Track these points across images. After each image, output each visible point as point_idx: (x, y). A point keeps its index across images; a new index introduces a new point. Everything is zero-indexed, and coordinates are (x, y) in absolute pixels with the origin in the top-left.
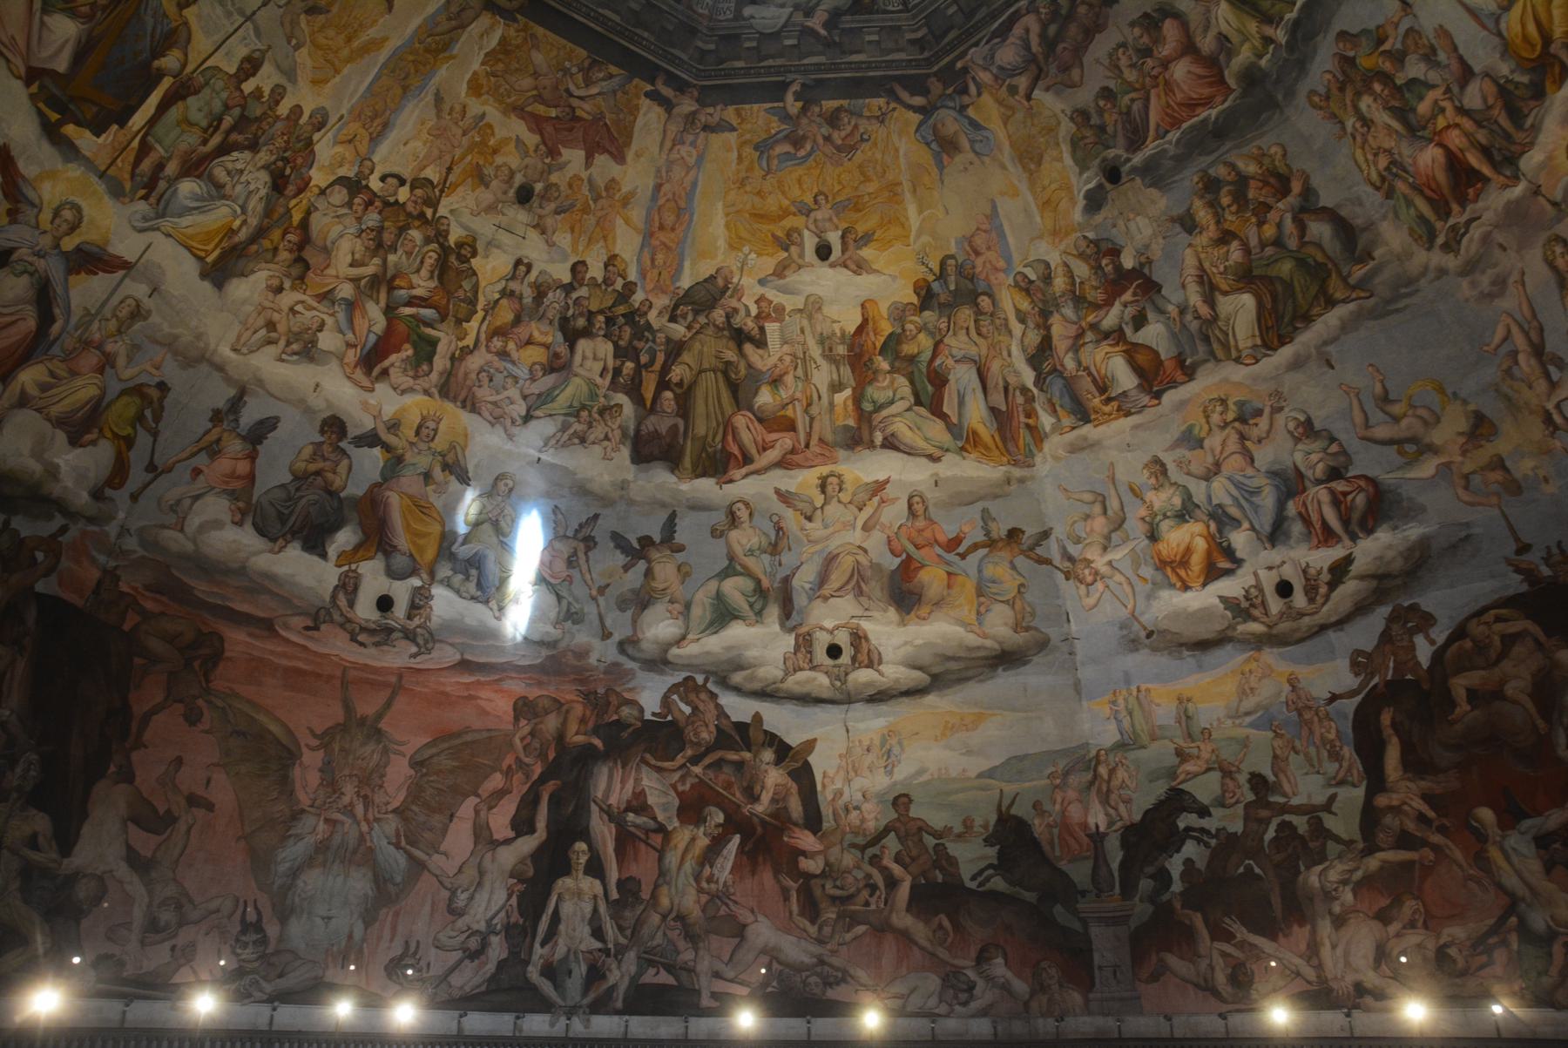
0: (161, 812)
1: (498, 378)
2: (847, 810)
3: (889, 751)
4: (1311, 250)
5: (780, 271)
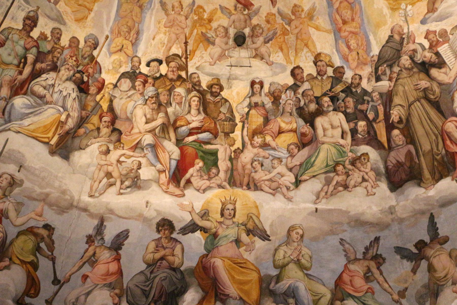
1: (267, 162)
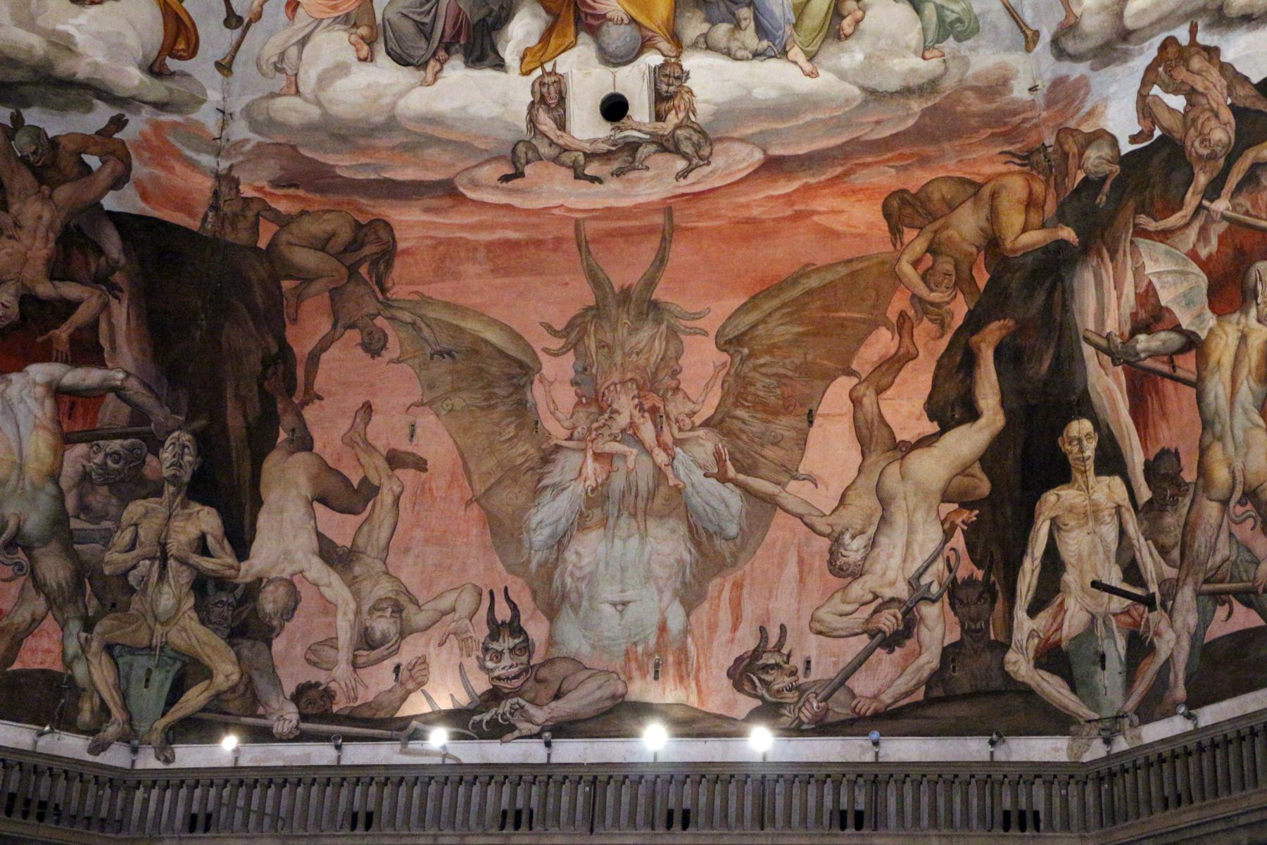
0: (356, 485)
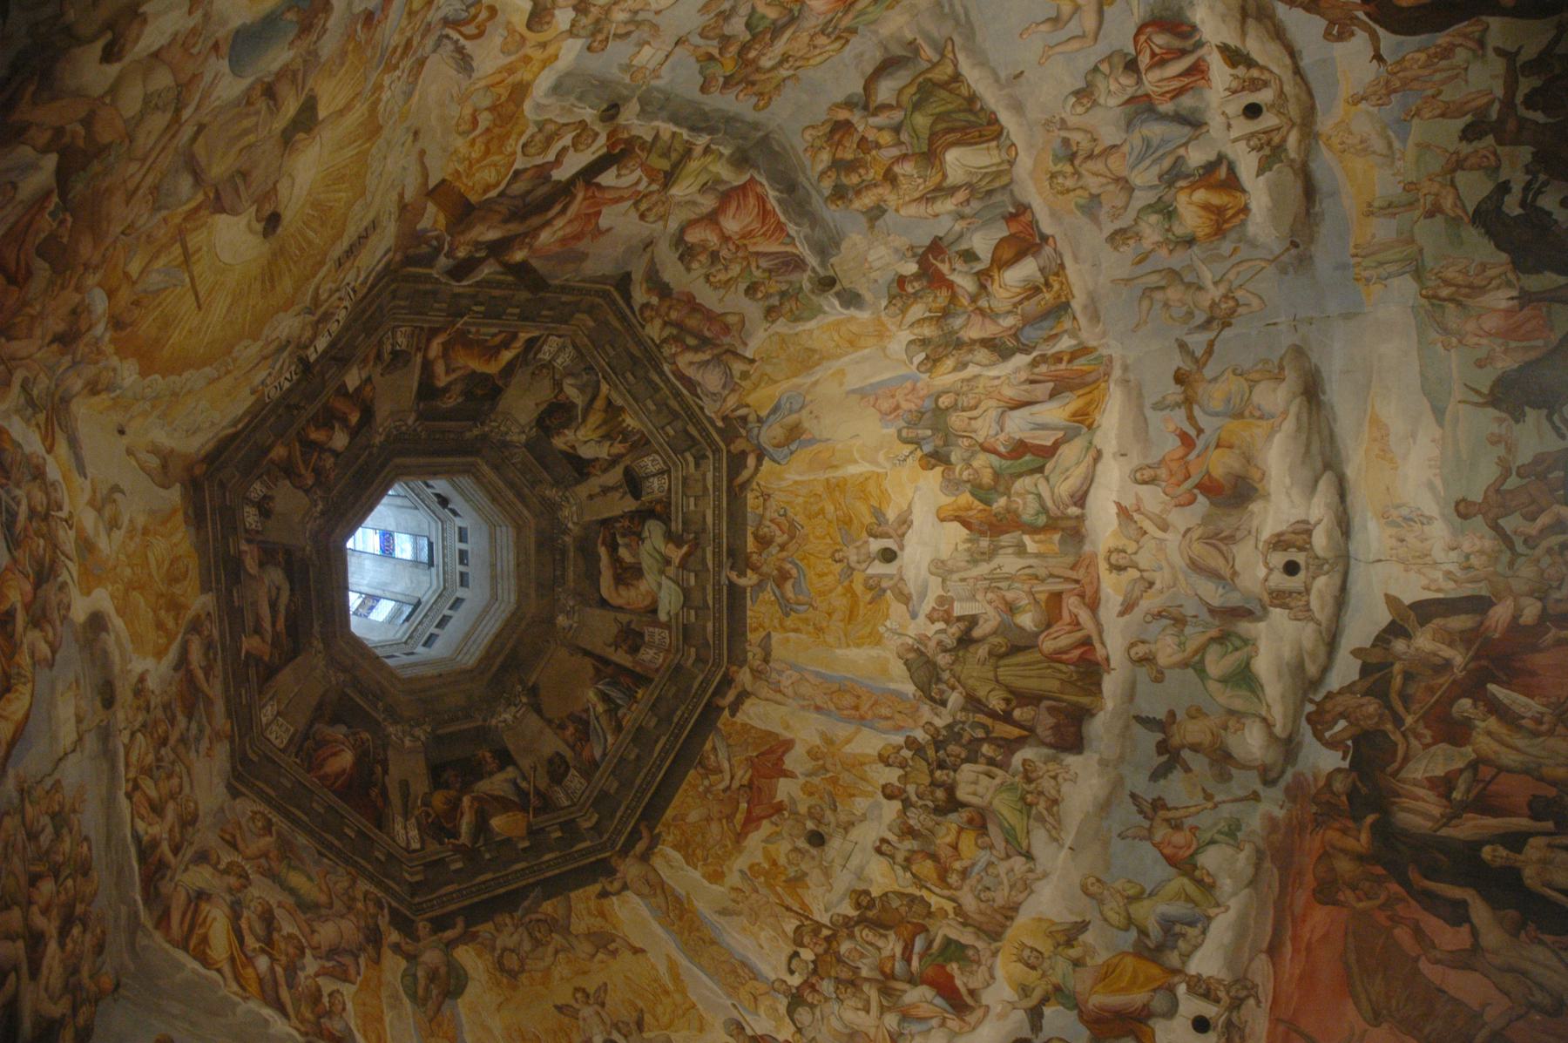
1: (987, 881)
2: (1469, 568)
3: (1406, 519)
4: (905, 99)
5: (905, 598)
